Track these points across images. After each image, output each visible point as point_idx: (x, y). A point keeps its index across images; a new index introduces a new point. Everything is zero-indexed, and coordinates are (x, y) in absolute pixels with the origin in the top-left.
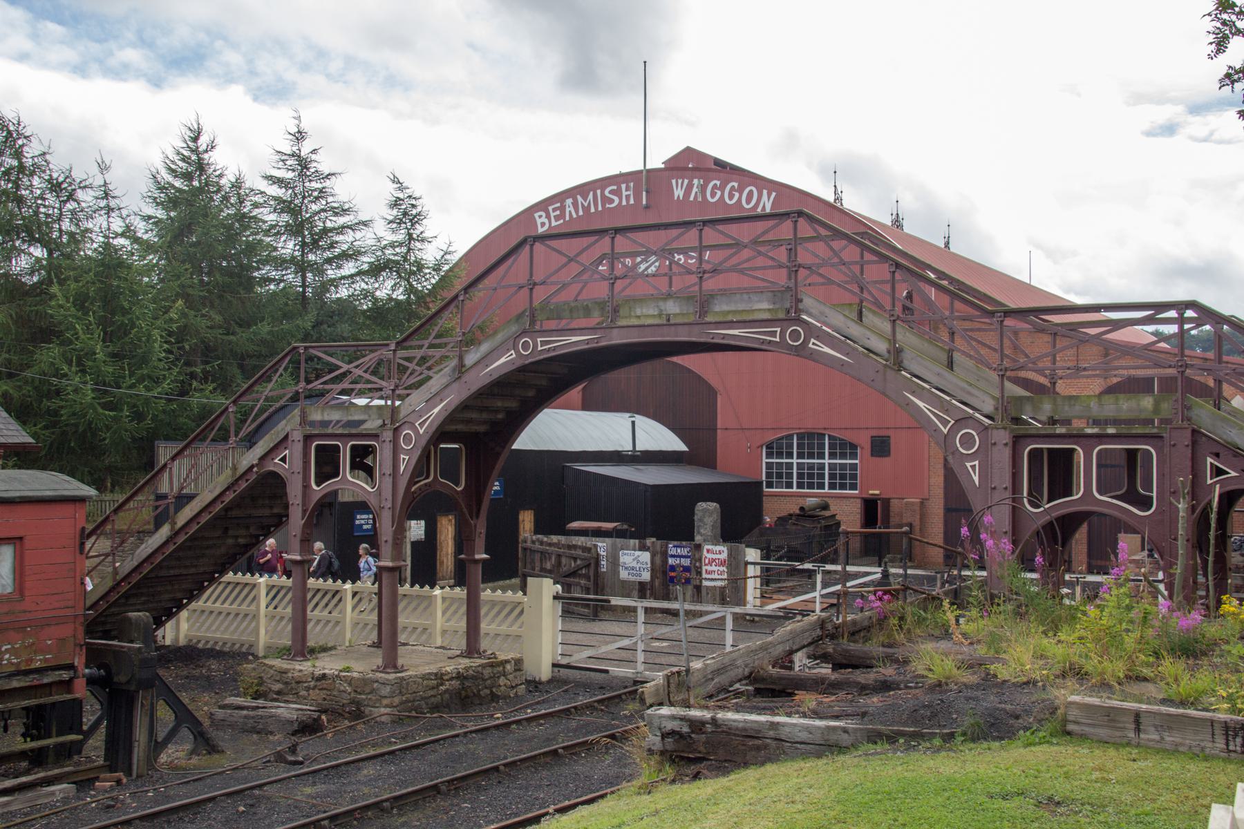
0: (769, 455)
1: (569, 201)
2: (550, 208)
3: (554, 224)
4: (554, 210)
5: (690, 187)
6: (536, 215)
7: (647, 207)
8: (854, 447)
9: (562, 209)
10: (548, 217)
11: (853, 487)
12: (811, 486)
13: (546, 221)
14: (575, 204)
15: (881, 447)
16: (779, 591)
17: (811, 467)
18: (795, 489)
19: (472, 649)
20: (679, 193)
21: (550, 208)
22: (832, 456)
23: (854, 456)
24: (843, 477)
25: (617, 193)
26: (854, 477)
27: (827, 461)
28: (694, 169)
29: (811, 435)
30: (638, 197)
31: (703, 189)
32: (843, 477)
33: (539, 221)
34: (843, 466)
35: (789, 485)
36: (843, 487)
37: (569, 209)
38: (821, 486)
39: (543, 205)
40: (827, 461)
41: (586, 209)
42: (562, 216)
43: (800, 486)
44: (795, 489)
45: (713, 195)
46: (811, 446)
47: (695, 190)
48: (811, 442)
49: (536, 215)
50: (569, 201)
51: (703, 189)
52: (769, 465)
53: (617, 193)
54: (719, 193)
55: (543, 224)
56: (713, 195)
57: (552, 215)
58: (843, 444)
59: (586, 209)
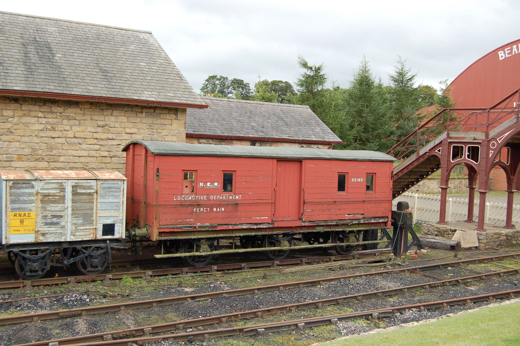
1: (515, 47)
2: (506, 50)
3: (507, 56)
4: (508, 50)
6: (499, 53)
9: (511, 50)
10: (505, 53)
13: (504, 55)
19: (509, 224)
21: (506, 50)
33: (500, 55)
42: (511, 53)
49: (499, 53)
50: (515, 47)
55: (502, 56)
57: (506, 52)
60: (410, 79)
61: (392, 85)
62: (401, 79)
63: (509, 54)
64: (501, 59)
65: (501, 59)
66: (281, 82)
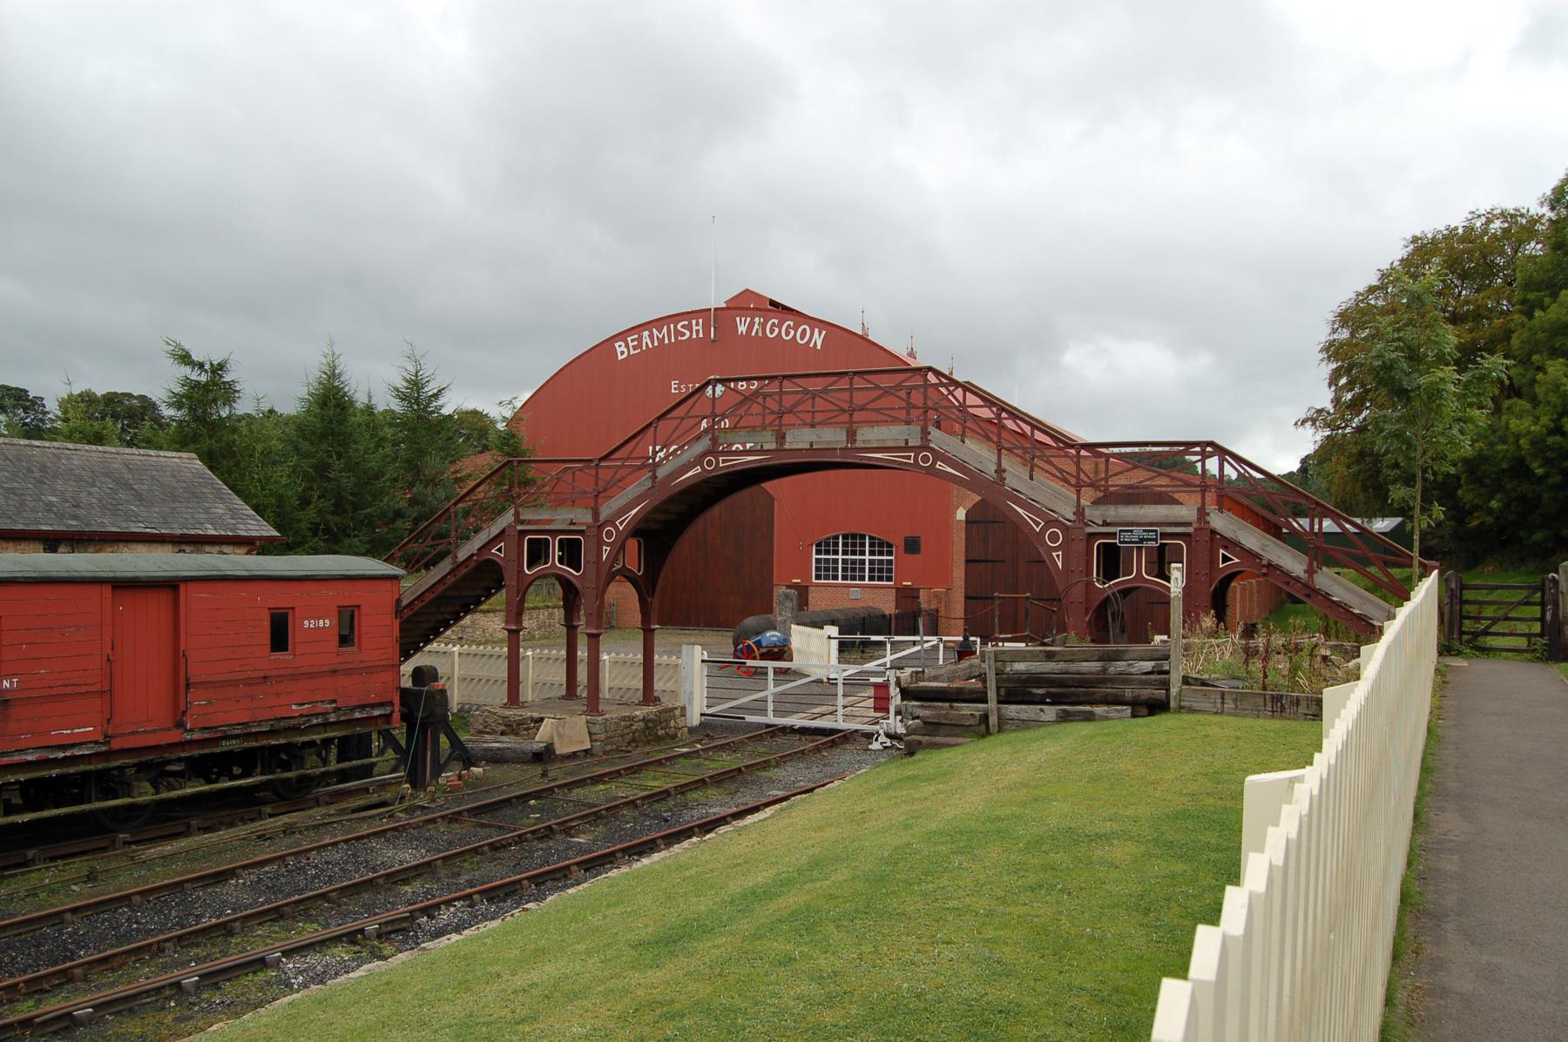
0: (818, 552)
1: (646, 333)
8: (890, 546)
9: (640, 340)
10: (627, 346)
11: (889, 579)
12: (853, 578)
14: (651, 336)
15: (912, 546)
17: (854, 562)
19: (649, 696)
20: (742, 329)
22: (872, 553)
23: (889, 553)
24: (881, 570)
25: (689, 327)
26: (890, 571)
27: (867, 557)
28: (755, 309)
29: (854, 536)
31: (763, 326)
32: (881, 570)
34: (881, 562)
35: (835, 577)
36: (880, 579)
38: (862, 578)
39: (622, 336)
40: (867, 557)
41: (661, 341)
42: (639, 346)
43: (844, 578)
45: (772, 331)
48: (854, 541)
50: (646, 333)
51: (763, 326)
52: (818, 561)
53: (689, 327)
56: (772, 331)
58: (881, 545)
59: (661, 341)
60: (436, 396)
61: (397, 406)
62: (415, 392)
63: (635, 348)
66: (130, 396)
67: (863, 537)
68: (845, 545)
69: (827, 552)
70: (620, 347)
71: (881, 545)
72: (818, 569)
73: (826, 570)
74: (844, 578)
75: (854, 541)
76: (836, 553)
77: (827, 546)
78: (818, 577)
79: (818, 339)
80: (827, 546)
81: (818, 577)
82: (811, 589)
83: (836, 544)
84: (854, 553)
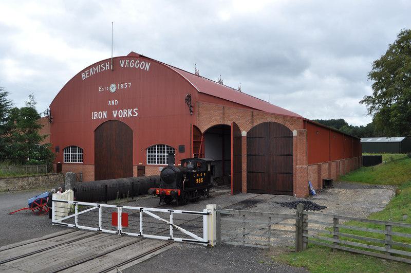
1: (91, 69)
3: (87, 77)
5: (125, 62)
7: (113, 70)
8: (174, 149)
9: (89, 72)
10: (85, 75)
12: (161, 163)
14: (93, 70)
16: (221, 188)
18: (156, 164)
20: (122, 65)
25: (105, 66)
29: (161, 145)
30: (110, 67)
31: (129, 63)
33: (83, 76)
37: (91, 72)
39: (83, 71)
43: (158, 163)
44: (156, 164)
45: (132, 65)
46: (161, 149)
47: (127, 63)
50: (91, 69)
51: (129, 63)
52: (149, 156)
53: (105, 66)
54: (134, 64)
57: (87, 74)
64: (83, 79)
65: (83, 79)
67: (164, 146)
68: (158, 149)
69: (152, 152)
70: (83, 75)
71: (171, 149)
72: (149, 159)
73: (152, 159)
74: (158, 163)
75: (161, 147)
76: (155, 152)
77: (151, 150)
78: (149, 162)
79: (148, 67)
80: (151, 150)
81: (149, 162)
82: (146, 167)
83: (155, 149)
84: (161, 153)
